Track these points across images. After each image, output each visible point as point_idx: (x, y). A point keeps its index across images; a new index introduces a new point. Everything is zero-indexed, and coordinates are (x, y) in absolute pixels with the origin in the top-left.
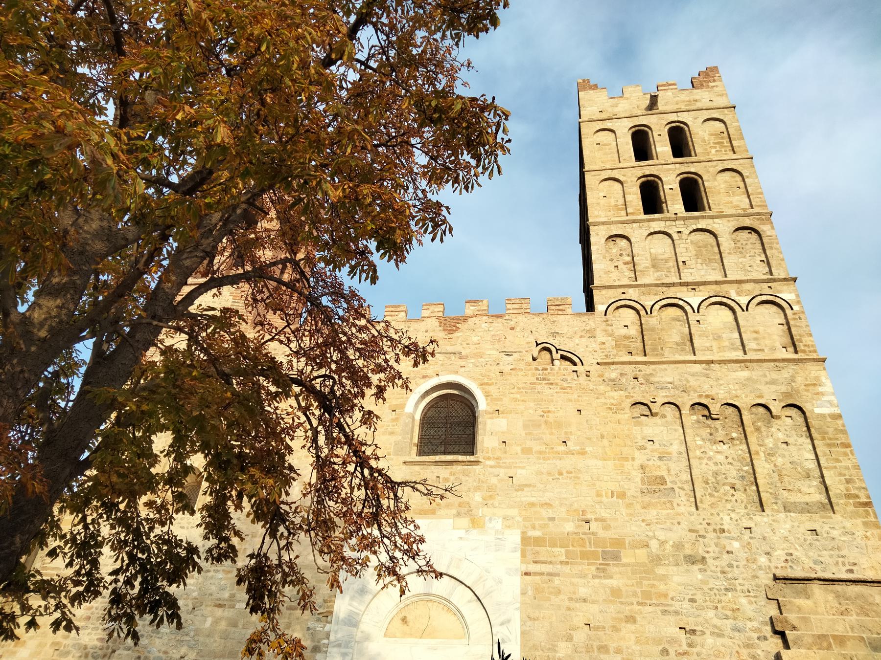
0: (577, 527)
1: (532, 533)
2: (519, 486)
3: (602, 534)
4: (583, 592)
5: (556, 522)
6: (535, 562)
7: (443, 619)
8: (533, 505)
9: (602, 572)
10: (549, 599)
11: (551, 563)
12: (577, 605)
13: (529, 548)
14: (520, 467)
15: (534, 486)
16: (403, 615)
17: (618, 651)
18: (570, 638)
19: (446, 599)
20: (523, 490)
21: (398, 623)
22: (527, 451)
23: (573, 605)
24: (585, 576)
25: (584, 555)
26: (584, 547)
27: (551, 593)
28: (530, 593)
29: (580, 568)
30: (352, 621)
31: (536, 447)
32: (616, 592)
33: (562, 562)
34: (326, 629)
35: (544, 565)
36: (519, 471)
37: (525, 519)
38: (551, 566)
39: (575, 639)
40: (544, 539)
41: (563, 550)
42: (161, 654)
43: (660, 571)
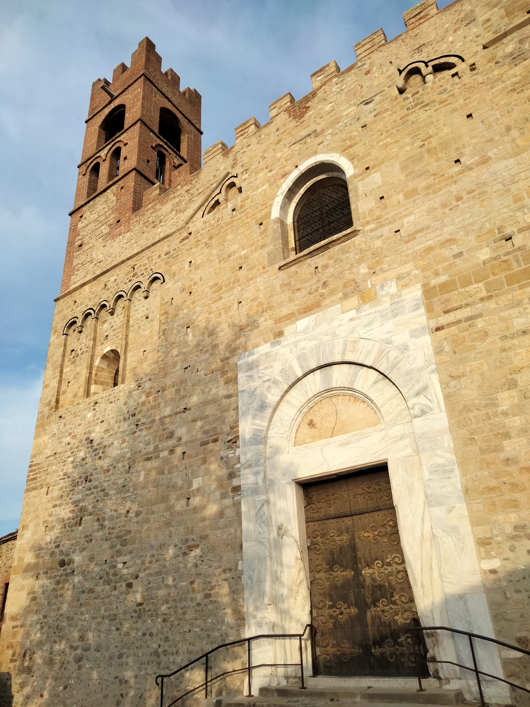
0: (494, 250)
1: (435, 282)
2: (409, 236)
5: (465, 256)
6: (447, 312)
8: (430, 249)
10: (474, 348)
11: (467, 305)
12: (516, 342)
13: (436, 299)
14: (406, 216)
15: (428, 228)
16: (309, 418)
18: (513, 385)
19: (349, 389)
20: (414, 238)
21: (305, 429)
22: (411, 194)
23: (507, 344)
24: (519, 304)
25: (511, 280)
26: (510, 269)
27: (475, 340)
28: (447, 349)
29: (510, 296)
30: (260, 439)
31: (421, 183)
33: (482, 299)
34: (237, 454)
35: (459, 311)
36: (406, 220)
37: (423, 269)
38: (469, 309)
39: (520, 383)
40: (453, 282)
41: (481, 285)
42: (113, 513)
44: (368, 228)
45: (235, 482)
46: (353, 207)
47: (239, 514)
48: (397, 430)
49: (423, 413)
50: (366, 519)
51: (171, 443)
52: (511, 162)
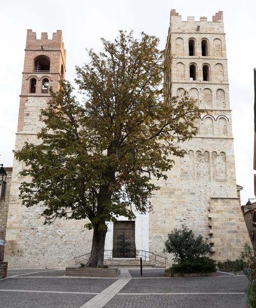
3: (170, 187)
4: (164, 201)
9: (170, 197)
17: (172, 215)
18: (161, 212)
25: (165, 193)
32: (173, 202)
43: (184, 196)
50: (127, 231)
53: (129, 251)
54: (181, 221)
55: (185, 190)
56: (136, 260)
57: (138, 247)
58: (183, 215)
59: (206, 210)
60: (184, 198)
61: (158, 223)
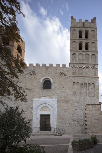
1: (59, 99)
4: (65, 106)
7: (47, 109)
8: (59, 96)
9: (67, 104)
17: (68, 112)
18: (63, 111)
25: (65, 102)
32: (68, 106)
37: (58, 97)
43: (74, 103)
44: (53, 90)
45: (32, 113)
46: (52, 86)
47: (32, 116)
48: (52, 112)
49: (55, 111)
51: (22, 107)
52: (68, 90)
53: (47, 128)
54: (72, 115)
55: (74, 100)
56: (50, 132)
57: (51, 126)
58: (73, 112)
59: (84, 109)
60: (74, 104)
61: (61, 116)
